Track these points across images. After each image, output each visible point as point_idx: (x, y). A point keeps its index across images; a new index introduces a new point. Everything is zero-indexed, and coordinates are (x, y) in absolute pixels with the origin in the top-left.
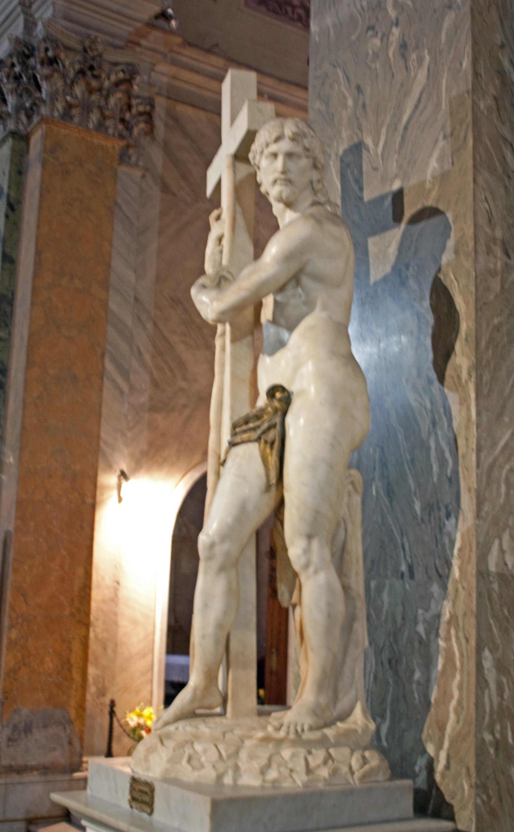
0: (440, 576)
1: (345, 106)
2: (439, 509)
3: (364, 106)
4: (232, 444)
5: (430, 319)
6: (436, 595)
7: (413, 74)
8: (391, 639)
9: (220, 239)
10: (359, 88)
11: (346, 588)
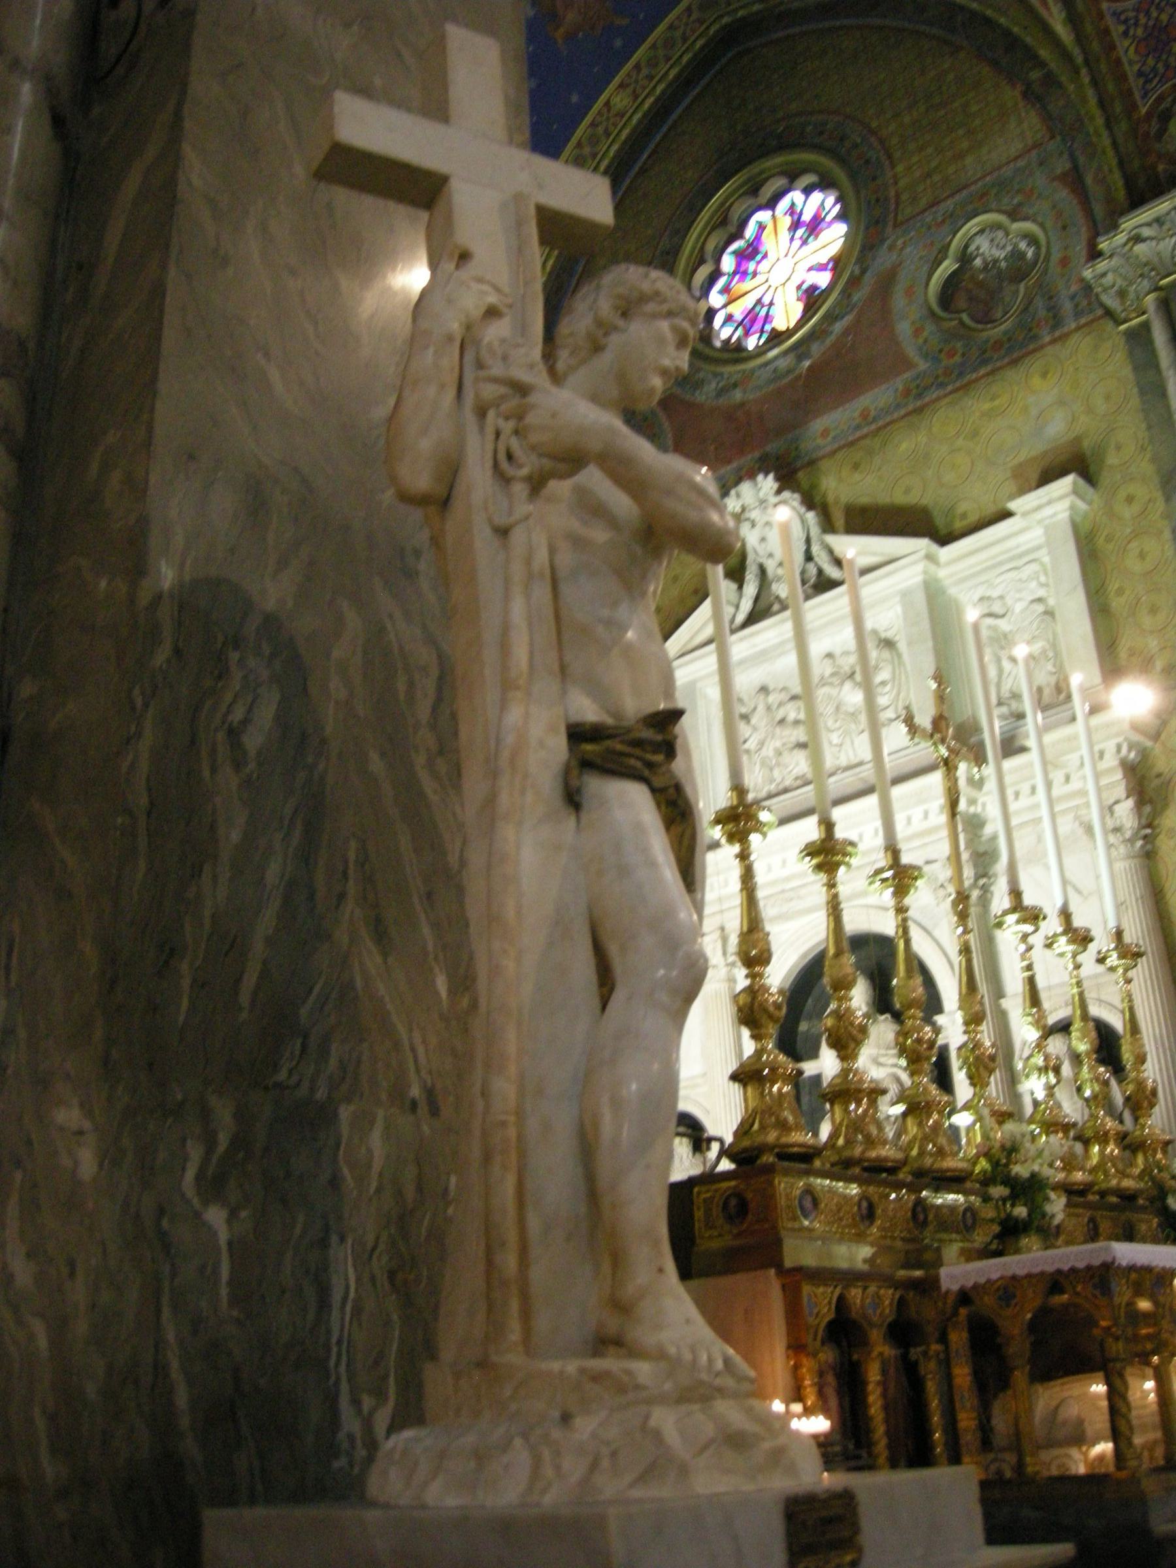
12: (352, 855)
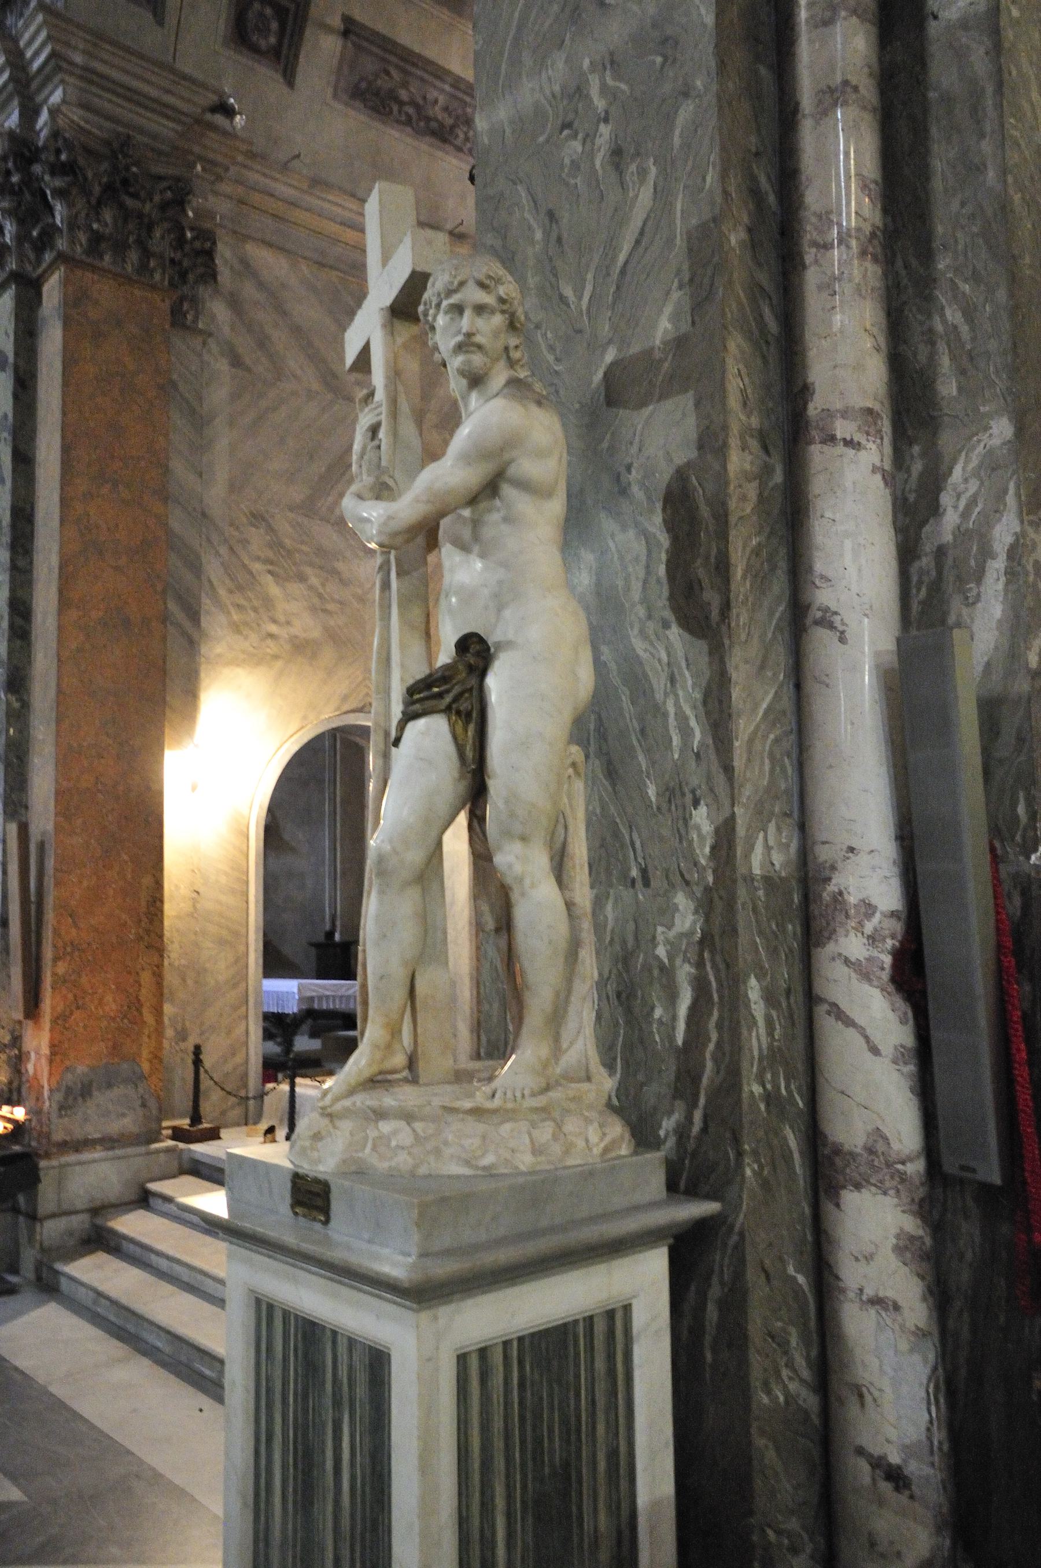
0: (687, 883)
1: (532, 242)
2: (683, 795)
3: (559, 240)
4: (409, 716)
5: (664, 539)
6: (680, 907)
7: (631, 194)
8: (620, 966)
9: (374, 430)
10: (551, 215)
11: (569, 905)
12: (592, 727)
